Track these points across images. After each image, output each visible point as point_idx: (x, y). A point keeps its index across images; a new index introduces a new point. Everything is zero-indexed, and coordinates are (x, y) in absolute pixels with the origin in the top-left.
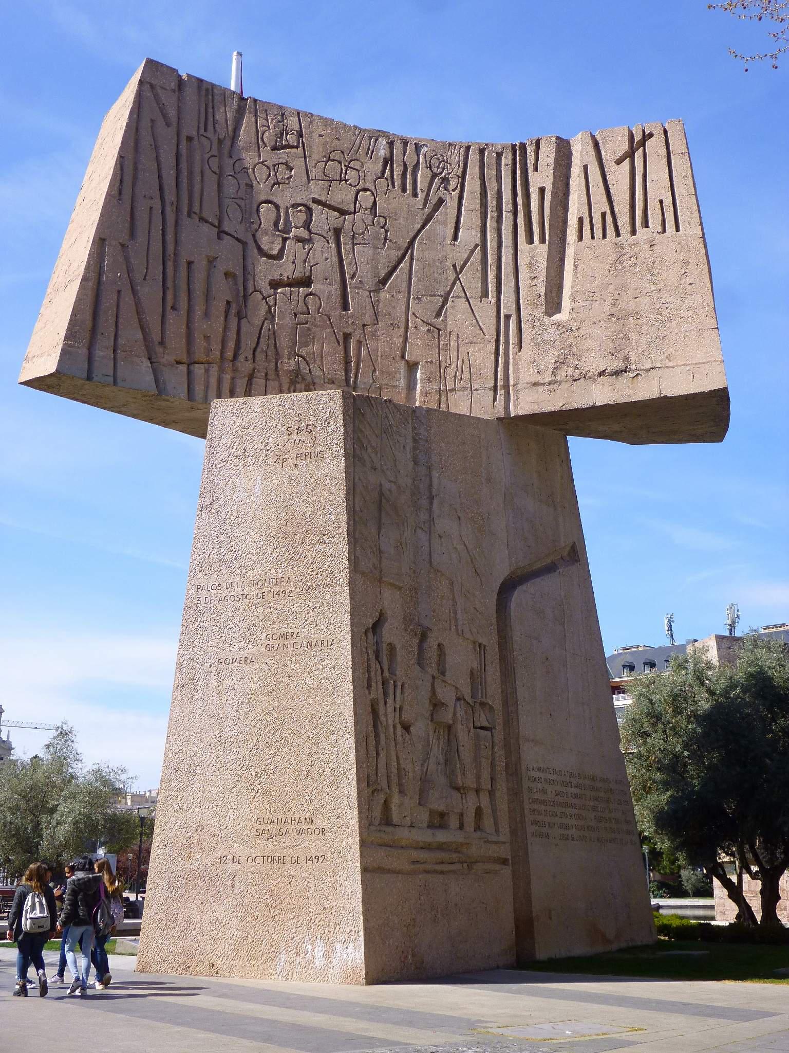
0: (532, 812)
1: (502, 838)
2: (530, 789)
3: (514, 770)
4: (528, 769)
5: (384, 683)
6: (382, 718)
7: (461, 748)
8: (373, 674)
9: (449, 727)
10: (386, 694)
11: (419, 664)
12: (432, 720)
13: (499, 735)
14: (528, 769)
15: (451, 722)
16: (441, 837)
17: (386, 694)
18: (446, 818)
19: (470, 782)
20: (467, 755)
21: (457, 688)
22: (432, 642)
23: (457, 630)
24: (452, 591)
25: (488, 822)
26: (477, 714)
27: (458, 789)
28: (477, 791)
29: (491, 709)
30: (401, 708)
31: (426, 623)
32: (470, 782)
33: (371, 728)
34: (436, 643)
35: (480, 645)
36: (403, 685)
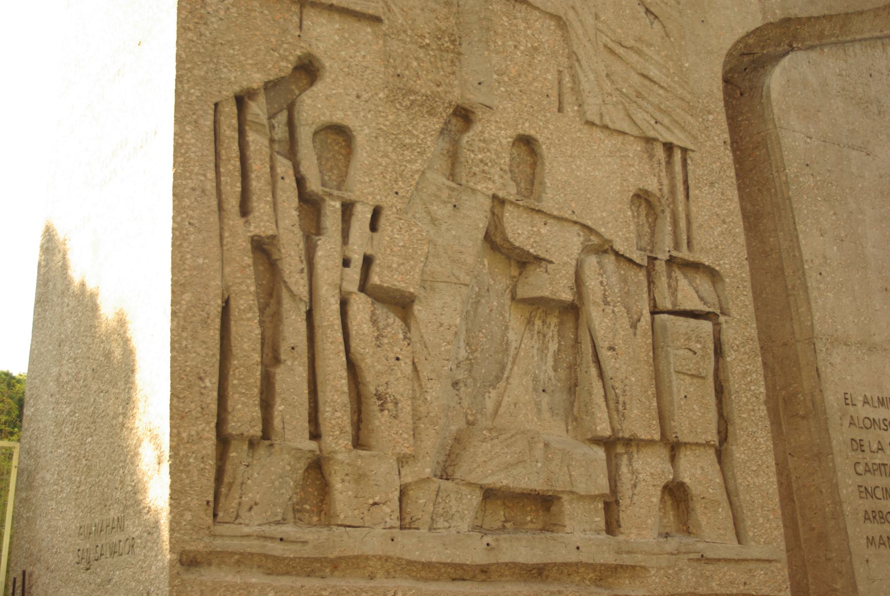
0: (867, 492)
1: (754, 550)
2: (858, 445)
3: (792, 403)
4: (848, 401)
5: (310, 204)
6: (297, 282)
7: (604, 354)
8: (259, 184)
9: (573, 311)
10: (312, 227)
11: (452, 176)
12: (513, 298)
13: (741, 330)
14: (848, 401)
15: (567, 296)
16: (524, 549)
17: (312, 227)
18: (554, 509)
19: (640, 422)
20: (627, 365)
21: (585, 227)
22: (493, 135)
23: (581, 112)
24: (566, 39)
25: (711, 520)
26: (662, 281)
27: (609, 444)
28: (674, 448)
29: (713, 274)
30: (368, 261)
31: (474, 97)
32: (640, 422)
33: (246, 305)
34: (506, 137)
35: (669, 147)
36: (376, 213)
